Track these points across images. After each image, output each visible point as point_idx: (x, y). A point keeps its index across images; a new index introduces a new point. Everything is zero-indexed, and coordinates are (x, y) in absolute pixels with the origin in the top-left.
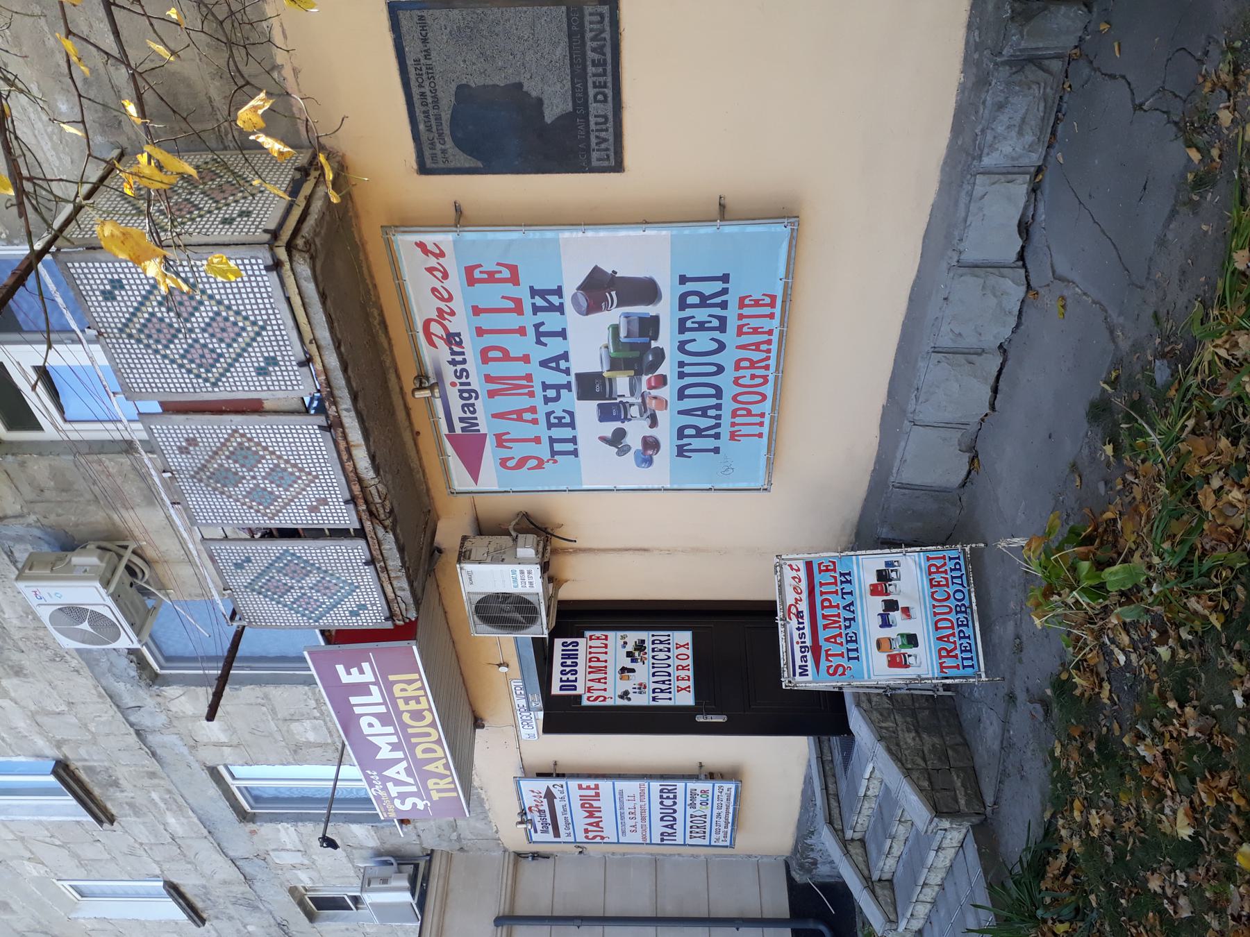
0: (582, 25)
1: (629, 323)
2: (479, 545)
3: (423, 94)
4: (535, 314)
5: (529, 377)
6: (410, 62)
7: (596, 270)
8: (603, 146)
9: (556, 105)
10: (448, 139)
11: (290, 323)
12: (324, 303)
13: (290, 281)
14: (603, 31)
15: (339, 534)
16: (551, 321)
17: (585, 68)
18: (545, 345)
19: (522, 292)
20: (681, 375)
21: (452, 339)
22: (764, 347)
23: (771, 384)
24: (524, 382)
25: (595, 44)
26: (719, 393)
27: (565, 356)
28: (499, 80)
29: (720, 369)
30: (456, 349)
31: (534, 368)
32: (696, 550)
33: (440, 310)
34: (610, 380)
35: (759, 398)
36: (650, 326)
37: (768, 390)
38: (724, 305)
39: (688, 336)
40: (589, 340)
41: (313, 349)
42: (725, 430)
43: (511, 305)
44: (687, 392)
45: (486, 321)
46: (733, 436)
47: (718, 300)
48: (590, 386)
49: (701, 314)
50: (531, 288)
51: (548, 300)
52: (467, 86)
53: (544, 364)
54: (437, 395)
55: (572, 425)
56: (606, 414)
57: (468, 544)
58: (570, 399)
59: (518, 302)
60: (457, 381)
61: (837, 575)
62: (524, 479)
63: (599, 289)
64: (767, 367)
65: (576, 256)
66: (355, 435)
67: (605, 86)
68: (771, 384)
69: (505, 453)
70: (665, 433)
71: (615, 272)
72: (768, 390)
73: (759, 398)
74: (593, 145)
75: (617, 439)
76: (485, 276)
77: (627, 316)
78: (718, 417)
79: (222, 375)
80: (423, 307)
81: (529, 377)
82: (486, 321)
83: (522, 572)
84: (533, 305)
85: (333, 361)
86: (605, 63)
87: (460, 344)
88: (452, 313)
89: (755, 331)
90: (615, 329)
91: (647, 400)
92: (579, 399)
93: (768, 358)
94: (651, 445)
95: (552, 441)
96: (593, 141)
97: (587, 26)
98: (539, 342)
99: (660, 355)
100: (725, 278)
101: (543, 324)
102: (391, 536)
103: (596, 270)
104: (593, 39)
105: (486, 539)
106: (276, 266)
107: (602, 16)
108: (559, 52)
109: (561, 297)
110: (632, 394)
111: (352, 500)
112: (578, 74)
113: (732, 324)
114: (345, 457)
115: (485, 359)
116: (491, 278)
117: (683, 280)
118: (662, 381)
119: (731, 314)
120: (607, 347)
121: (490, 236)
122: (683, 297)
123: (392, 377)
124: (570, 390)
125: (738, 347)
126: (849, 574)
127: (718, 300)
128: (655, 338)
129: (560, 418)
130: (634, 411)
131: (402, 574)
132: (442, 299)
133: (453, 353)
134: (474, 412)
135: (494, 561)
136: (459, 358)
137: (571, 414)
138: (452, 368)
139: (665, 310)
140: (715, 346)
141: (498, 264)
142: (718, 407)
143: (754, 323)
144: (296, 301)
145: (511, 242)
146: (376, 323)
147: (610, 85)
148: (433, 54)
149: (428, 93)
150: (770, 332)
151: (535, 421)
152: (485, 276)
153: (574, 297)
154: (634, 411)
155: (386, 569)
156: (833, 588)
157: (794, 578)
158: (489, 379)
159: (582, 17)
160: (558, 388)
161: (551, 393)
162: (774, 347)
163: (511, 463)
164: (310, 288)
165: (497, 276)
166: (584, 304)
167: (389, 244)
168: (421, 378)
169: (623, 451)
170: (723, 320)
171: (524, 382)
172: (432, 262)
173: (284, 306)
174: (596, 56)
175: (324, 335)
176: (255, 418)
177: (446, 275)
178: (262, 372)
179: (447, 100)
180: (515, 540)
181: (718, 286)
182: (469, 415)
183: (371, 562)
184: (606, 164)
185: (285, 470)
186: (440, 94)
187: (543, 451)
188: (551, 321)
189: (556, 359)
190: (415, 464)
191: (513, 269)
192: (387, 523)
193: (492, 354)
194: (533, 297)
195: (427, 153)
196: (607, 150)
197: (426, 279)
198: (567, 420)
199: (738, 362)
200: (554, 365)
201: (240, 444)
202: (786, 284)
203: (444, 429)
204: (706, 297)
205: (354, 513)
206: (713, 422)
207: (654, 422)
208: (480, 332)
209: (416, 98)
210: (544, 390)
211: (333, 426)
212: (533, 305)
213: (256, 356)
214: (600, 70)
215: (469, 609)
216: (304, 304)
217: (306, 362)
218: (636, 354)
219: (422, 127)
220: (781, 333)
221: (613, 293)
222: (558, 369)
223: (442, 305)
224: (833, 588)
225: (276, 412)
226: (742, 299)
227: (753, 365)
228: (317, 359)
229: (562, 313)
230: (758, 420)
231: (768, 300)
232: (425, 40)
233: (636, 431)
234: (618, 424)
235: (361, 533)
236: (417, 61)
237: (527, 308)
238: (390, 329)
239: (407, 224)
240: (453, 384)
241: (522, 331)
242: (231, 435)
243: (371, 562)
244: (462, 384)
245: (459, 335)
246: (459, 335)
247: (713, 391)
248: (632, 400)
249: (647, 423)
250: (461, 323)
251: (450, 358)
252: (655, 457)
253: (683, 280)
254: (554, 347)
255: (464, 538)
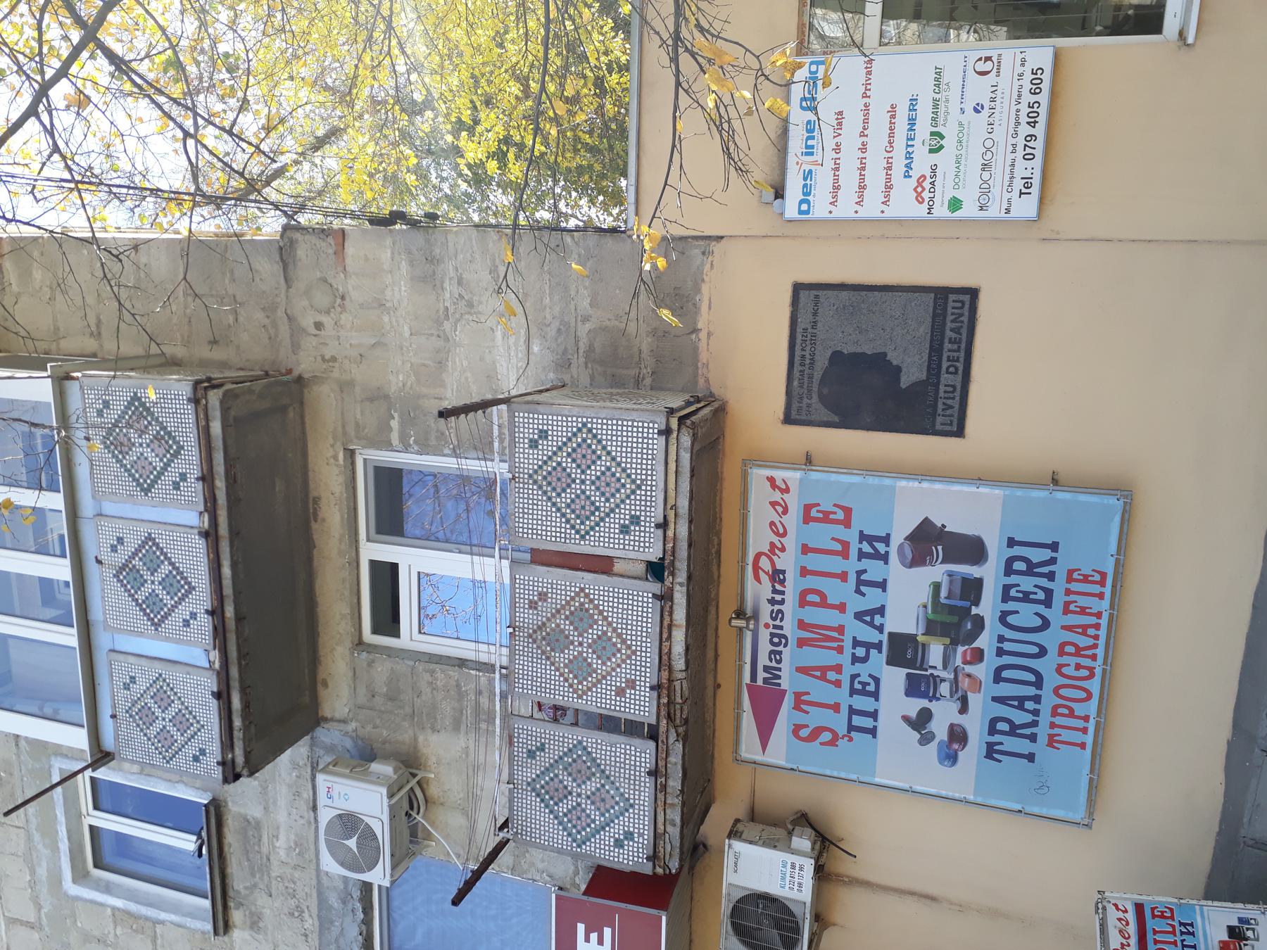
0: (945, 309)
1: (951, 582)
2: (752, 830)
3: (803, 356)
4: (859, 560)
5: (841, 629)
6: (799, 330)
7: (926, 521)
8: (948, 412)
9: (912, 372)
10: (815, 396)
11: (661, 485)
12: (692, 476)
13: (673, 449)
14: (962, 315)
15: (632, 729)
16: (874, 570)
17: (941, 344)
18: (864, 595)
19: (852, 536)
20: (1000, 652)
21: (777, 576)
22: (1091, 631)
23: (1097, 679)
24: (835, 634)
25: (954, 325)
26: (1039, 684)
27: (881, 611)
28: (868, 349)
29: (1043, 652)
30: (778, 587)
31: (848, 619)
32: (995, 914)
33: (772, 544)
34: (924, 645)
35: (1084, 695)
36: (972, 589)
37: (1094, 686)
38: (1051, 576)
39: (1011, 606)
40: (908, 596)
41: (671, 514)
42: (1042, 731)
43: (839, 547)
44: (1005, 674)
45: (814, 561)
46: (1052, 741)
47: (1045, 570)
48: (903, 650)
49: (1027, 583)
50: (861, 532)
51: (875, 546)
52: (840, 352)
53: (859, 616)
54: (751, 627)
55: (875, 695)
56: (915, 687)
57: (740, 827)
58: (878, 660)
59: (846, 545)
60: (771, 623)
61: (1176, 924)
62: (815, 758)
63: (927, 541)
64: (1094, 657)
65: (908, 506)
66: (680, 615)
67: (958, 360)
68: (1097, 679)
69: (800, 718)
70: (975, 724)
71: (944, 526)
72: (1094, 686)
73: (1084, 695)
74: (940, 411)
75: (920, 722)
76: (820, 515)
77: (951, 575)
78: (1036, 713)
79: (592, 528)
80: (759, 538)
81: (841, 629)
82: (814, 561)
83: (793, 866)
84: (860, 549)
85: (683, 530)
86: (960, 342)
87: (782, 582)
88: (783, 549)
89: (1083, 611)
90: (937, 587)
91: (960, 677)
92: (888, 663)
93: (1095, 646)
94: (958, 736)
95: (852, 711)
96: (940, 406)
97: (950, 310)
98: (858, 591)
99: (979, 623)
100: (1054, 547)
101: (865, 571)
102: (680, 746)
103: (926, 521)
104: (952, 321)
105: (761, 827)
106: (666, 432)
107: (963, 302)
108: (921, 330)
109: (888, 545)
110: (945, 667)
111: (656, 688)
112: (936, 349)
113: (1059, 599)
114: (665, 636)
115: (803, 603)
116: (826, 518)
117: (1012, 543)
118: (978, 656)
119: (1058, 586)
120: (925, 607)
121: (834, 477)
122: (1010, 561)
123: (713, 610)
124: (880, 652)
125: (1064, 628)
126: (1192, 924)
127: (1045, 570)
128: (977, 602)
129: (865, 684)
130: (944, 689)
131: (678, 801)
132: (777, 534)
133: (775, 591)
134: (779, 662)
135: (765, 845)
136: (778, 597)
137: (877, 681)
138: (770, 607)
139: (990, 573)
140: (1039, 622)
141: (835, 505)
142: (1037, 699)
143: (1083, 601)
144: (672, 466)
145: (853, 484)
146: (713, 551)
147: (962, 360)
148: (819, 325)
149: (808, 356)
150: (1099, 615)
151: (838, 684)
152: (820, 515)
153: (901, 547)
154: (944, 689)
155: (664, 787)
156: (1170, 938)
157: (1120, 920)
158: (802, 625)
159: (946, 304)
160: (868, 646)
161: (861, 652)
162: (1102, 633)
163: (804, 733)
164: (686, 457)
165: (832, 516)
166: (909, 555)
167: (745, 476)
168: (740, 614)
169: (926, 739)
170: (1049, 593)
171: (835, 634)
172: (777, 496)
173: (661, 468)
174: (954, 335)
175: (684, 503)
176: (604, 577)
177: (785, 511)
178: (625, 530)
179: (822, 362)
180: (790, 833)
181: (1046, 554)
182: (774, 664)
183: (654, 773)
184: (948, 428)
185: (610, 639)
186: (816, 358)
187: (839, 722)
188: (874, 570)
189: (872, 612)
190: (708, 717)
191: (848, 511)
192: (681, 730)
193: (810, 598)
194: (860, 542)
195: (795, 405)
196: (951, 416)
197: (766, 517)
198: (871, 688)
199: (1063, 645)
200: (868, 618)
201: (582, 604)
202: (1117, 561)
203: (747, 678)
204: (1033, 564)
205: (655, 703)
206: (1029, 718)
207: (964, 709)
208: (804, 572)
209: (797, 359)
210: (854, 648)
211: (665, 598)
212: (860, 549)
213: (623, 516)
214: (955, 347)
215: (725, 908)
216: (676, 472)
217: (663, 525)
218: (955, 619)
219: (796, 383)
220: (1111, 616)
221: (940, 548)
222: (871, 624)
223: (775, 539)
224: (1170, 938)
225: (622, 576)
226: (1071, 572)
227: (1078, 651)
228: (672, 526)
229: (886, 563)
230: (1080, 724)
231: (1097, 577)
232: (815, 314)
233: (944, 714)
234: (924, 703)
235: (653, 735)
236: (805, 330)
237: (853, 553)
238: (722, 564)
239: (763, 462)
240: (767, 626)
241: (843, 577)
242: (577, 594)
243: (654, 773)
244: (775, 627)
245: (783, 572)
246: (783, 572)
247: (1032, 678)
248: (943, 674)
249: (956, 706)
250: (788, 562)
251: (770, 596)
252: (960, 753)
253: (1012, 543)
254: (873, 598)
255: (737, 821)
